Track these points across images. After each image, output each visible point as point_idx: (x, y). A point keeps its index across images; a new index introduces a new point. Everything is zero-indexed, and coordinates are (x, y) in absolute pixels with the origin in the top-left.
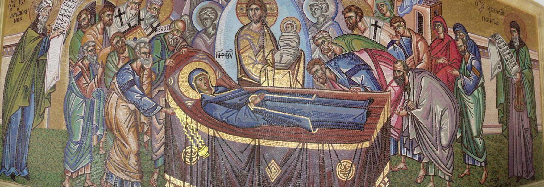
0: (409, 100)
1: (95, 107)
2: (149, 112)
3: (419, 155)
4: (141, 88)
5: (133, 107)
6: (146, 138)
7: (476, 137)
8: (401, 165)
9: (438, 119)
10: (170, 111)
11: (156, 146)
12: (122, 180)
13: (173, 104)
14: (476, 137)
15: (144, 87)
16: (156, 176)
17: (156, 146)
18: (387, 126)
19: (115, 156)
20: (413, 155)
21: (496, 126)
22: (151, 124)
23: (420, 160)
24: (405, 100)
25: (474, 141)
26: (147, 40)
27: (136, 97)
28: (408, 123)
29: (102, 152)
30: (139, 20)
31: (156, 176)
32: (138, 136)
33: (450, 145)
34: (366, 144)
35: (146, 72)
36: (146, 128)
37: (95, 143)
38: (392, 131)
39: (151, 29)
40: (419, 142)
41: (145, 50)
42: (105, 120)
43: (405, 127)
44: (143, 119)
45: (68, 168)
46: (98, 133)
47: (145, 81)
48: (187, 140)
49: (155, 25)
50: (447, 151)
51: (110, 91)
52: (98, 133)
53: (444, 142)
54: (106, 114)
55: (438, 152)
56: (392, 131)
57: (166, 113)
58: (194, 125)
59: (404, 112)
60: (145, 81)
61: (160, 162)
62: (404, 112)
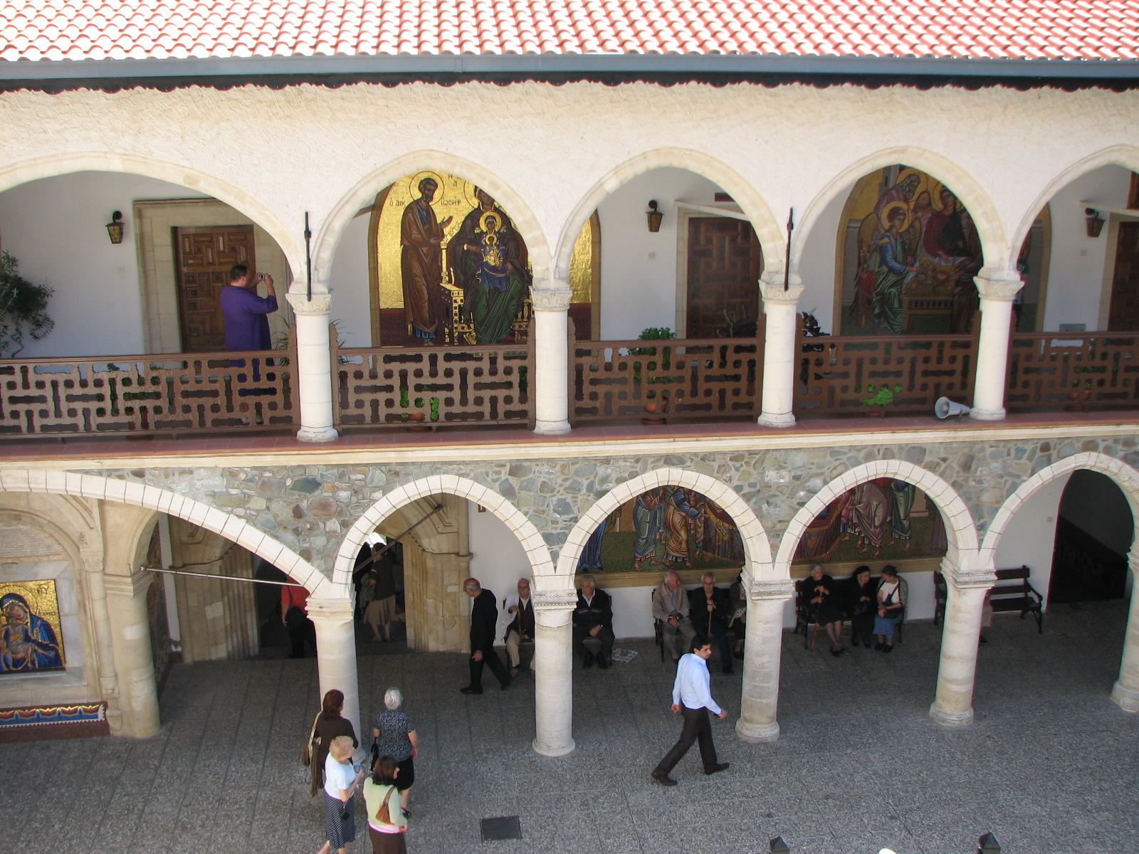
2: (694, 517)
4: (689, 503)
5: (684, 514)
6: (692, 532)
8: (847, 538)
9: (873, 510)
10: (707, 516)
13: (708, 511)
18: (840, 516)
19: (672, 544)
21: (924, 512)
22: (695, 524)
23: (859, 534)
25: (901, 523)
27: (686, 508)
28: (853, 515)
32: (688, 531)
33: (881, 526)
34: (827, 527)
40: (860, 524)
42: (665, 523)
44: (690, 521)
47: (692, 499)
48: (716, 532)
51: (668, 504)
53: (877, 524)
54: (666, 519)
59: (850, 507)
60: (692, 499)
61: (701, 545)
62: (850, 507)
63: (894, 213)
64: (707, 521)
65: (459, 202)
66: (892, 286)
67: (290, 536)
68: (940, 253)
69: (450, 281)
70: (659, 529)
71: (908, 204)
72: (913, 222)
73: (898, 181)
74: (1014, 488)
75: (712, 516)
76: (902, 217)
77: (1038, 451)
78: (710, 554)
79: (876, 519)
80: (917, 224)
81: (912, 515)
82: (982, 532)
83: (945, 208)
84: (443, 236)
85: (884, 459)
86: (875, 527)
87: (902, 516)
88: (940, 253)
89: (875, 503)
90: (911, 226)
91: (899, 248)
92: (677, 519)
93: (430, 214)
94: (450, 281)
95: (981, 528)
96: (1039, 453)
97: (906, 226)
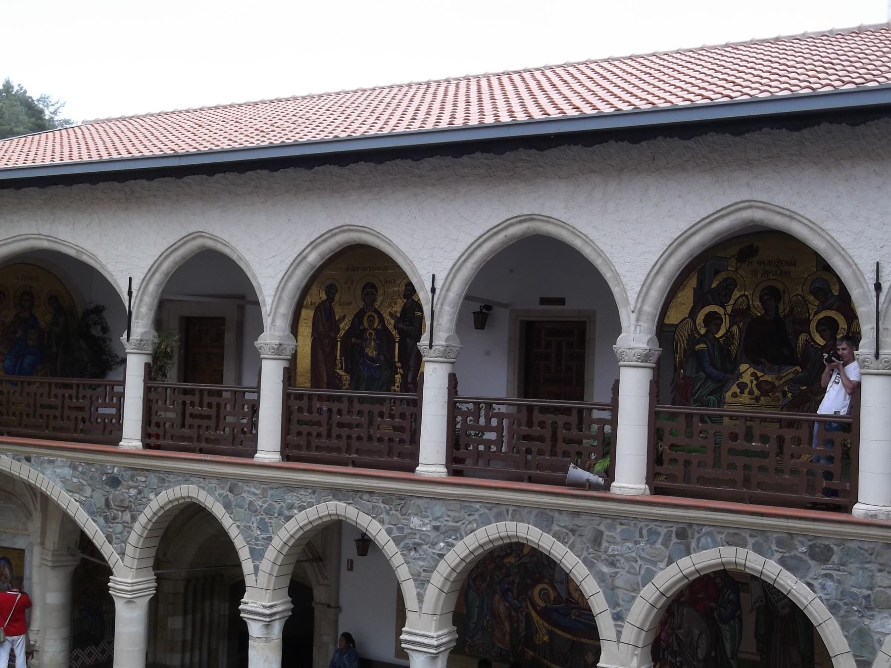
0: (674, 623)
1: (486, 601)
3: (681, 662)
4: (512, 593)
5: (508, 605)
6: (515, 625)
7: (731, 658)
11: (521, 630)
12: (501, 649)
14: (731, 658)
15: (515, 594)
16: (520, 648)
17: (521, 630)
20: (676, 661)
24: (671, 623)
26: (517, 565)
29: (490, 630)
30: (512, 550)
31: (520, 648)
35: (516, 585)
36: (515, 619)
37: (485, 624)
38: (662, 643)
39: (518, 558)
41: (515, 570)
43: (671, 641)
44: (513, 613)
45: (468, 639)
46: (487, 618)
48: (537, 630)
49: (521, 556)
50: (702, 664)
52: (487, 618)
53: (700, 657)
55: (695, 663)
56: (662, 643)
57: (527, 613)
58: (541, 622)
62: (670, 631)
63: (712, 320)
64: (528, 617)
65: (351, 303)
66: (710, 394)
67: (101, 520)
68: (763, 360)
69: (341, 368)
70: (486, 616)
71: (724, 308)
72: (730, 327)
73: (714, 286)
74: (649, 577)
75: (534, 614)
76: (718, 322)
77: (674, 535)
78: (532, 653)
79: (699, 651)
80: (735, 329)
81: (740, 655)
82: (620, 623)
83: (766, 313)
84: (339, 330)
85: (512, 520)
86: (698, 660)
87: (729, 655)
88: (763, 360)
89: (697, 632)
90: (727, 331)
91: (717, 354)
92: (502, 608)
93: (331, 313)
94: (341, 368)
95: (618, 617)
96: (674, 540)
97: (722, 332)
